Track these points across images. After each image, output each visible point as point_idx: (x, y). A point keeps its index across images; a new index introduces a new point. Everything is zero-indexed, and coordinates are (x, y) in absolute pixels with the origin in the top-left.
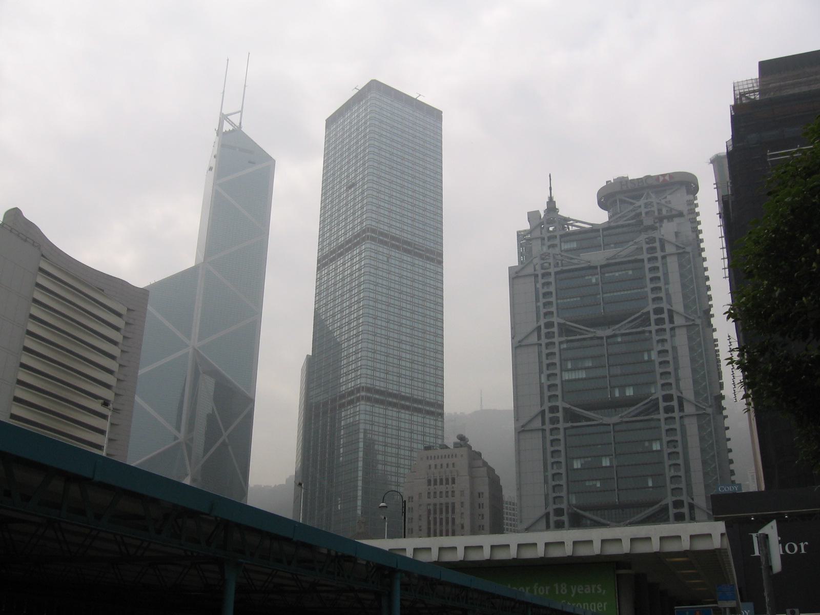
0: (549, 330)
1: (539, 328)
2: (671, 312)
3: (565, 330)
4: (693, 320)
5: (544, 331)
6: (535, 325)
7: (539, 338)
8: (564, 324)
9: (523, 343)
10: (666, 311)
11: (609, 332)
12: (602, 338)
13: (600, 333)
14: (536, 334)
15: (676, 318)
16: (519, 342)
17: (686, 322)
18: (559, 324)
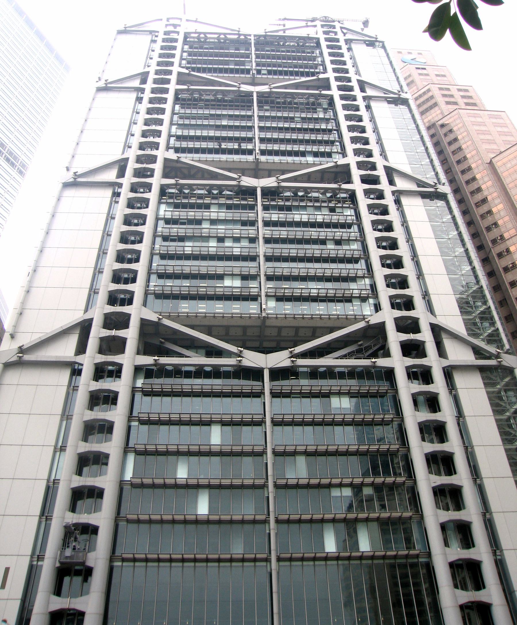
0: (113, 333)
1: (85, 327)
2: (437, 330)
3: (154, 338)
4: (498, 356)
5: (97, 332)
6: (78, 316)
7: (81, 349)
8: (157, 325)
9: (27, 357)
10: (425, 326)
11: (280, 359)
12: (256, 374)
13: (252, 359)
14: (73, 340)
15: (448, 344)
16: (22, 350)
17: (476, 359)
18: (144, 323)
